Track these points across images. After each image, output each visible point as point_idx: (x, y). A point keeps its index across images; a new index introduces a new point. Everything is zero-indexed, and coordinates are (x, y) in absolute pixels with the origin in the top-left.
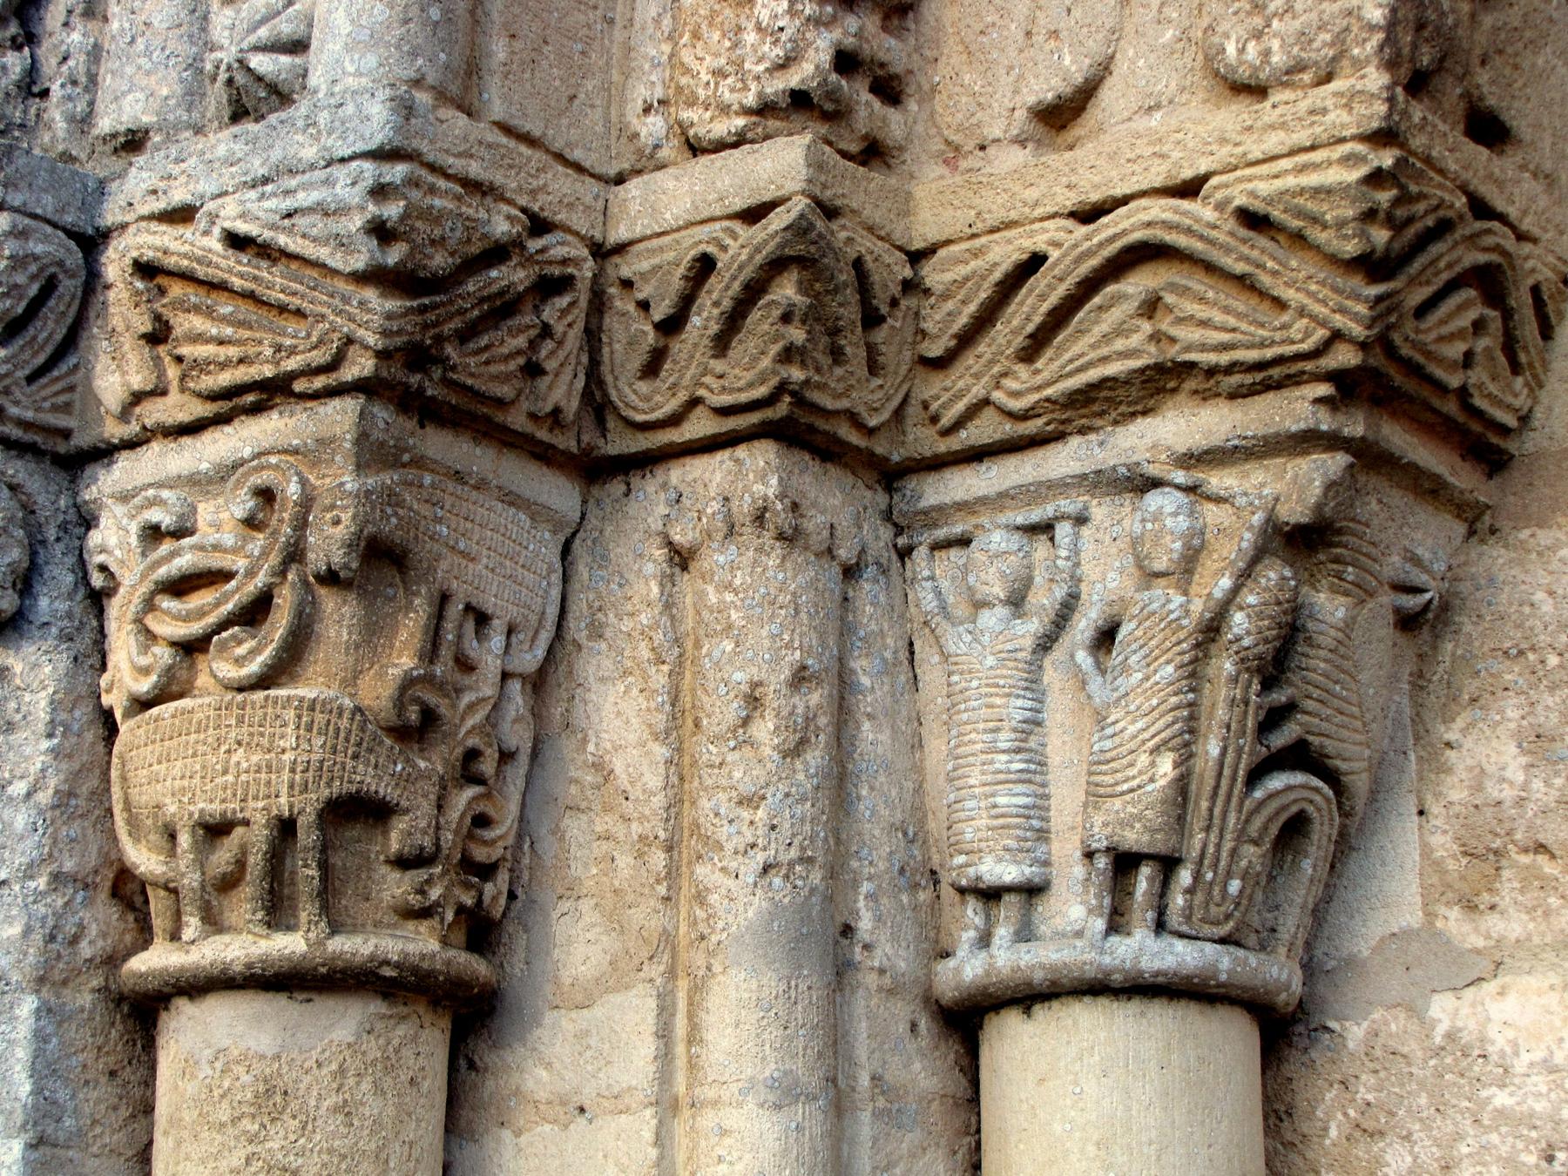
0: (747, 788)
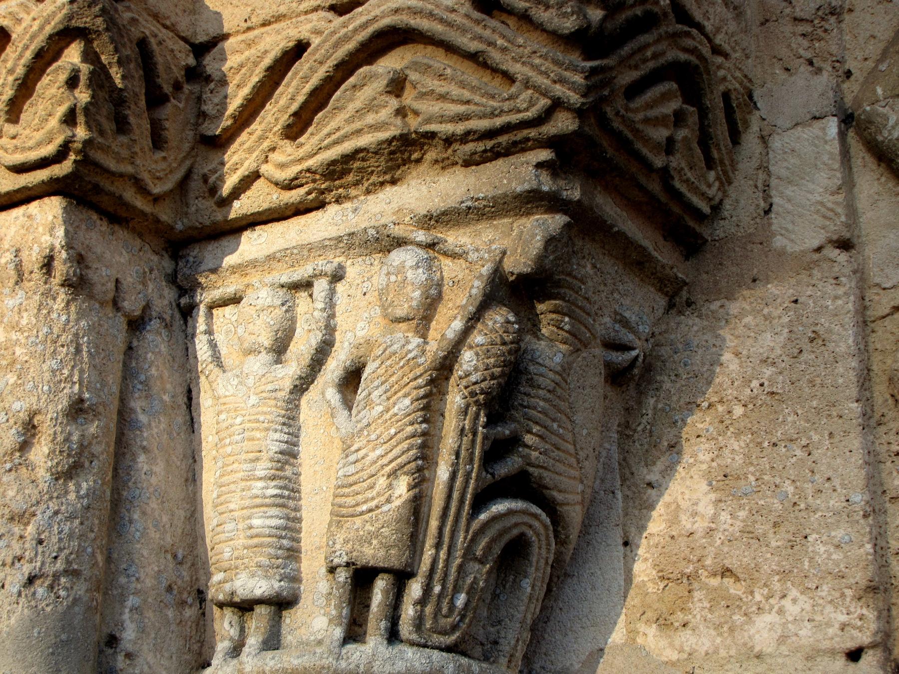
0: (19, 505)
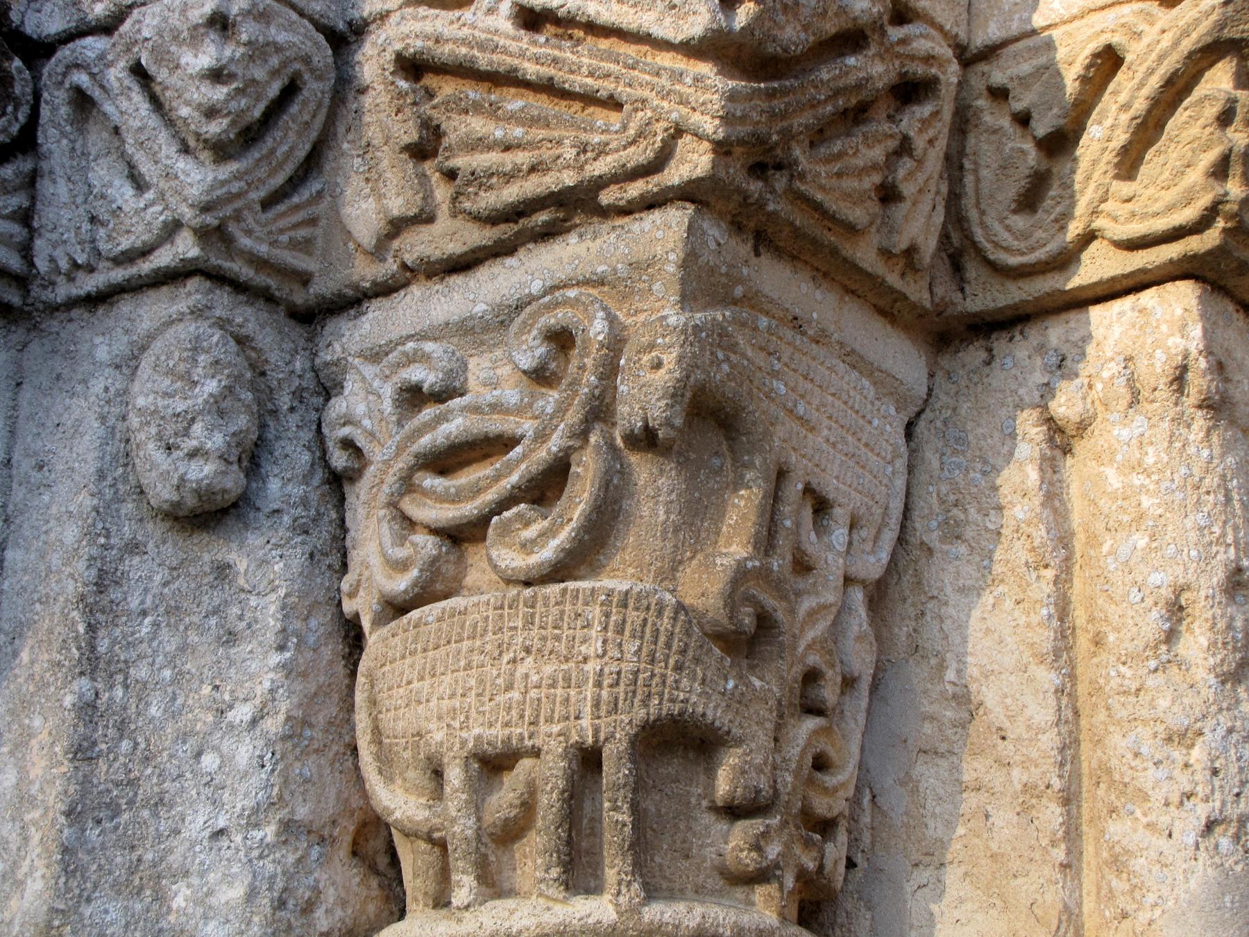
0: (1178, 721)
